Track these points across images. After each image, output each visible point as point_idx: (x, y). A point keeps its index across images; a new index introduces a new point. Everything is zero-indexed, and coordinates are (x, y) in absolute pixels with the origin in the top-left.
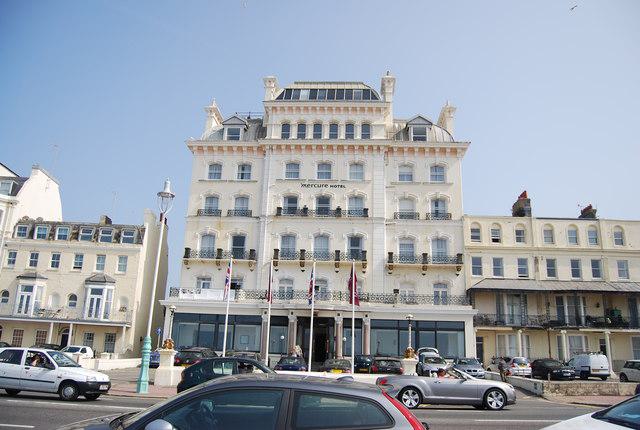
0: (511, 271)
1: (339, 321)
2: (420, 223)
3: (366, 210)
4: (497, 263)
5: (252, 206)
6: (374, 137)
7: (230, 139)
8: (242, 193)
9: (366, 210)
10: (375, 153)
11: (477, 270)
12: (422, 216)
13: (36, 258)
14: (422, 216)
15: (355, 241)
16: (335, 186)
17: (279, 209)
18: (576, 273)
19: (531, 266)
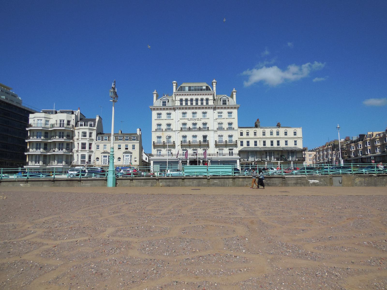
0: (252, 145)
3: (208, 128)
4: (248, 142)
11: (242, 145)
12: (225, 129)
13: (99, 147)
14: (225, 129)
15: (205, 137)
16: (198, 120)
17: (181, 128)
18: (272, 144)
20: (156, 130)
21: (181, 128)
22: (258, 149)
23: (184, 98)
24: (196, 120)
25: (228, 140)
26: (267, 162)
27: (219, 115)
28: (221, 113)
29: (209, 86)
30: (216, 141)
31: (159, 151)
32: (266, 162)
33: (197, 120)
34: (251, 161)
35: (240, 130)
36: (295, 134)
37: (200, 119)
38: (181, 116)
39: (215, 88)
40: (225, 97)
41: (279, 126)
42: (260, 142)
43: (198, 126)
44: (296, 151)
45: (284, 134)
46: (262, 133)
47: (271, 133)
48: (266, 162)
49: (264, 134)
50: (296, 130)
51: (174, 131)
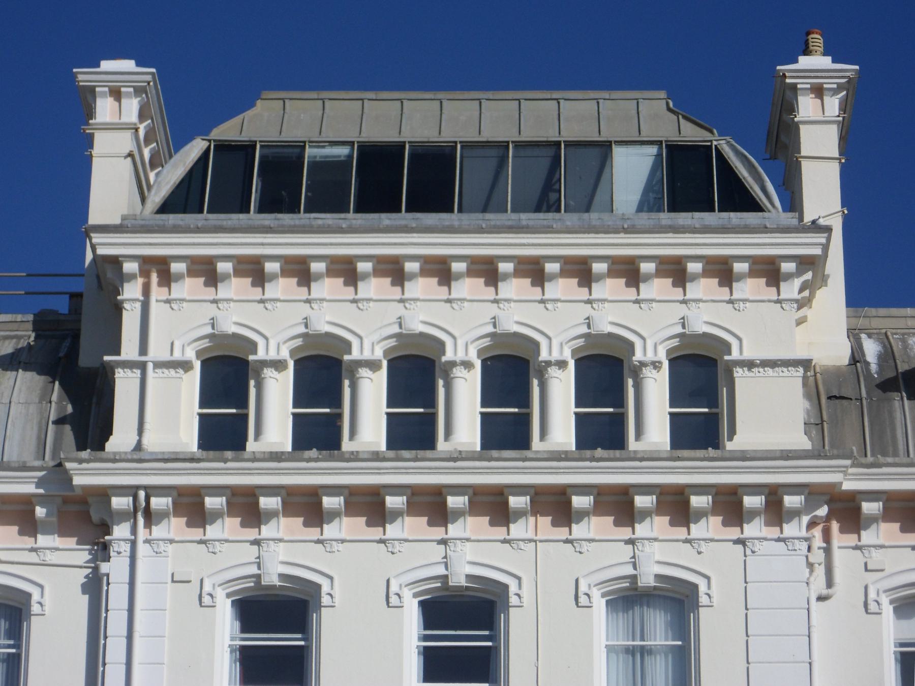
6: (742, 440)
10: (754, 529)
29: (725, 146)
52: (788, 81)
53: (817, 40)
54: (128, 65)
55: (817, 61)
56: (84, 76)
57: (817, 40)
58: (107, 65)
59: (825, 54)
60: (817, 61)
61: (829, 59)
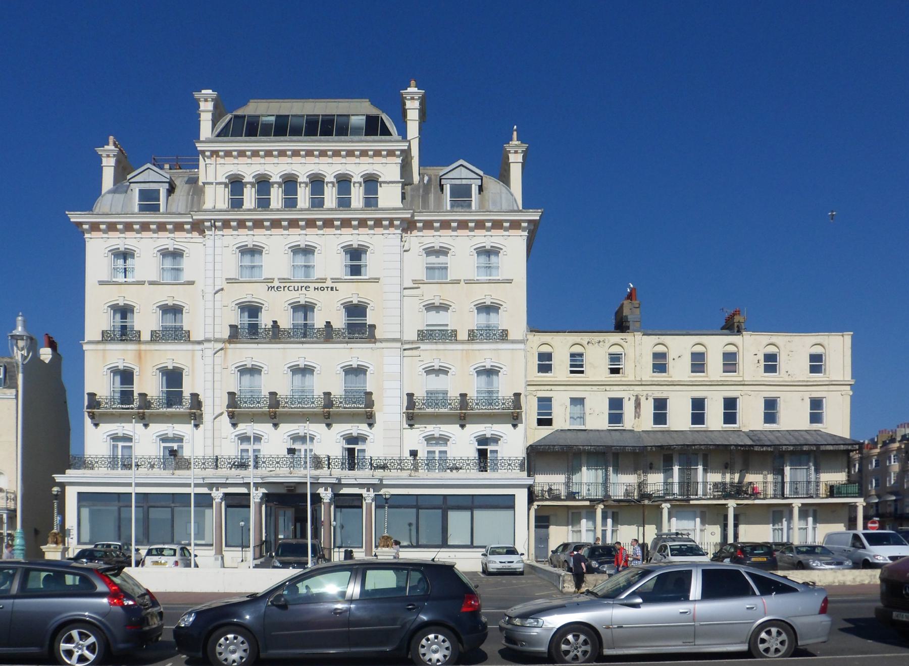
1: (326, 495)
2: (459, 347)
3: (373, 327)
5: (187, 322)
7: (143, 208)
8: (170, 303)
9: (373, 327)
16: (322, 289)
17: (233, 327)
18: (698, 418)
19: (628, 409)
20: (107, 337)
21: (233, 327)
22: (630, 442)
23: (249, 170)
24: (312, 286)
25: (472, 394)
26: (668, 505)
27: (433, 259)
28: (443, 252)
30: (410, 396)
31: (120, 444)
32: (664, 505)
33: (317, 285)
34: (591, 500)
35: (538, 342)
36: (816, 363)
37: (329, 284)
38: (230, 264)
39: (413, 129)
40: (464, 173)
41: (731, 327)
42: (638, 405)
43: (318, 321)
44: (823, 448)
45: (762, 363)
46: (649, 361)
47: (698, 362)
48: (664, 505)
49: (660, 363)
50: (825, 344)
51: (199, 343)
52: (404, 96)
53: (413, 83)
54: (210, 91)
55: (412, 89)
56: (197, 95)
57: (413, 83)
58: (204, 91)
59: (415, 87)
60: (412, 89)
61: (417, 89)
